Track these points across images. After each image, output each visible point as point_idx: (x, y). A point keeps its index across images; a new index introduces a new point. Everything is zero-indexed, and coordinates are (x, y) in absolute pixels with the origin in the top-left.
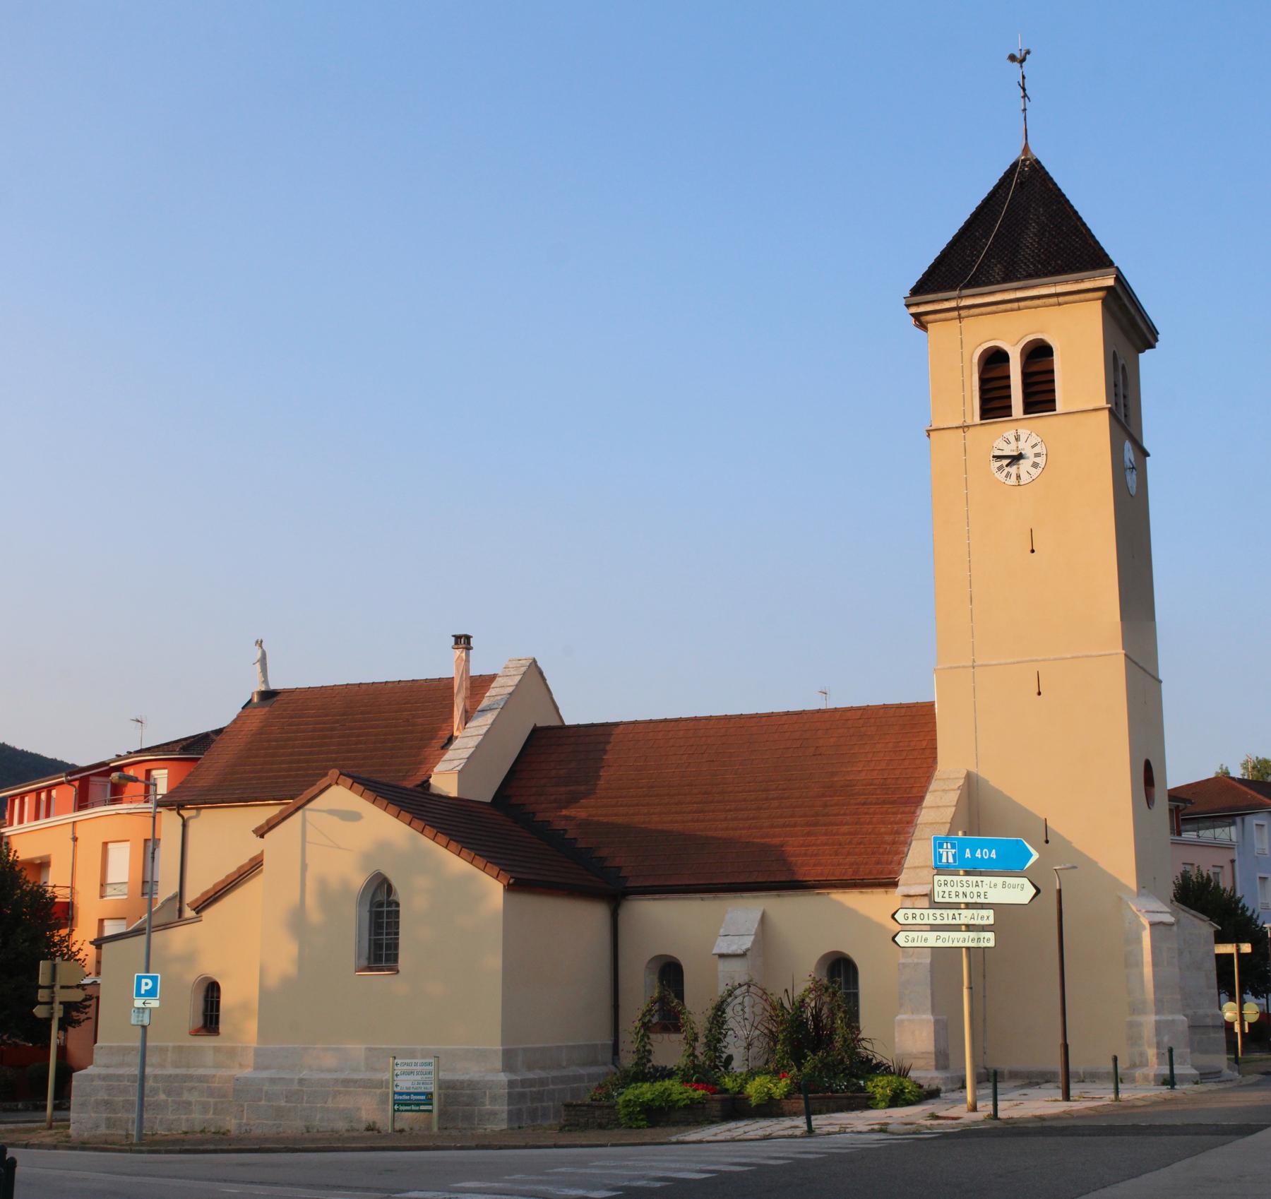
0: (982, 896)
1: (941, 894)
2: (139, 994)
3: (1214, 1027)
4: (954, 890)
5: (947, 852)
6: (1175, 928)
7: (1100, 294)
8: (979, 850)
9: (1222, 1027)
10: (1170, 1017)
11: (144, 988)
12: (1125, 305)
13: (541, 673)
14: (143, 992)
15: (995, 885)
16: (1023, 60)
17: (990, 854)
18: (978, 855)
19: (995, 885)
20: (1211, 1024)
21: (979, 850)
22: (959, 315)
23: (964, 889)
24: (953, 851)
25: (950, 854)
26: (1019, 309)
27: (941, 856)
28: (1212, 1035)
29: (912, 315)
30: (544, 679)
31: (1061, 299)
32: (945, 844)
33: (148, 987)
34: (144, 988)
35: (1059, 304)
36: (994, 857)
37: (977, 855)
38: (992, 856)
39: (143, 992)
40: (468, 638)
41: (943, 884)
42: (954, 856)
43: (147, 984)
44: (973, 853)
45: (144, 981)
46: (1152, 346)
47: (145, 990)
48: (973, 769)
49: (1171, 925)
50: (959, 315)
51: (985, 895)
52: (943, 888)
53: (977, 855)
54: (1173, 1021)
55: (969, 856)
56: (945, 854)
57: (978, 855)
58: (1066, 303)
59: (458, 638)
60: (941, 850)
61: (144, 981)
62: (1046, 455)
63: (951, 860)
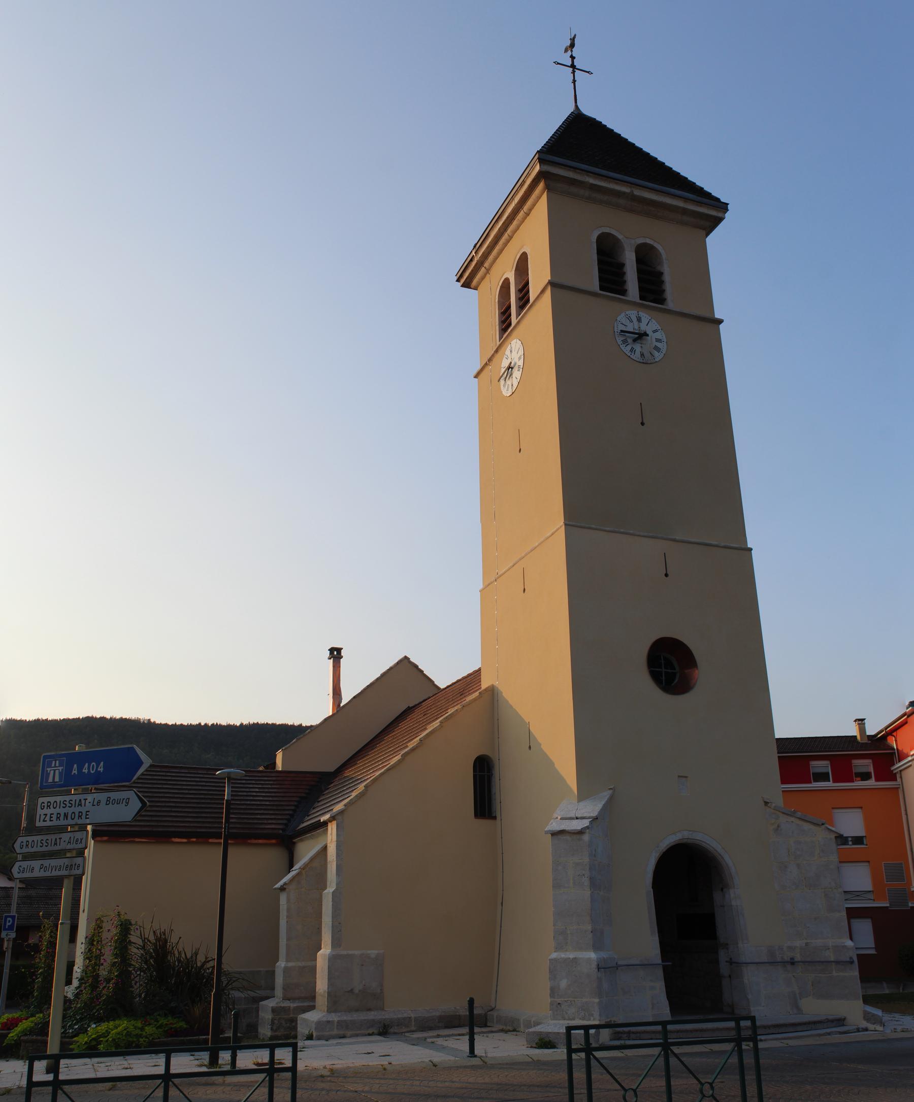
0: (83, 817)
1: (42, 817)
2: (5, 929)
3: (837, 962)
4: (55, 811)
5: (55, 770)
6: (586, 837)
7: (541, 185)
8: (87, 764)
9: (852, 962)
10: (571, 955)
11: (8, 924)
12: (592, 185)
13: (416, 667)
14: (7, 927)
15: (99, 802)
16: (572, 45)
17: (97, 768)
18: (85, 771)
19: (99, 802)
20: (832, 960)
21: (87, 765)
22: (485, 268)
23: (67, 810)
24: (61, 768)
25: (57, 772)
26: (511, 237)
27: (48, 775)
28: (835, 974)
29: (462, 286)
30: (422, 671)
31: (526, 208)
32: (54, 762)
33: (10, 924)
34: (8, 924)
35: (527, 214)
36: (102, 770)
37: (84, 771)
38: (99, 770)
39: (7, 927)
40: (339, 650)
41: (46, 807)
42: (60, 774)
43: (9, 921)
44: (80, 769)
45: (8, 919)
46: (718, 221)
47: (8, 926)
48: (496, 683)
49: (581, 832)
50: (485, 268)
51: (87, 815)
52: (46, 811)
53: (84, 771)
54: (575, 960)
55: (76, 772)
56: (52, 772)
57: (85, 771)
58: (530, 210)
59: (332, 650)
60: (49, 769)
61: (8, 919)
62: (524, 354)
63: (57, 779)
